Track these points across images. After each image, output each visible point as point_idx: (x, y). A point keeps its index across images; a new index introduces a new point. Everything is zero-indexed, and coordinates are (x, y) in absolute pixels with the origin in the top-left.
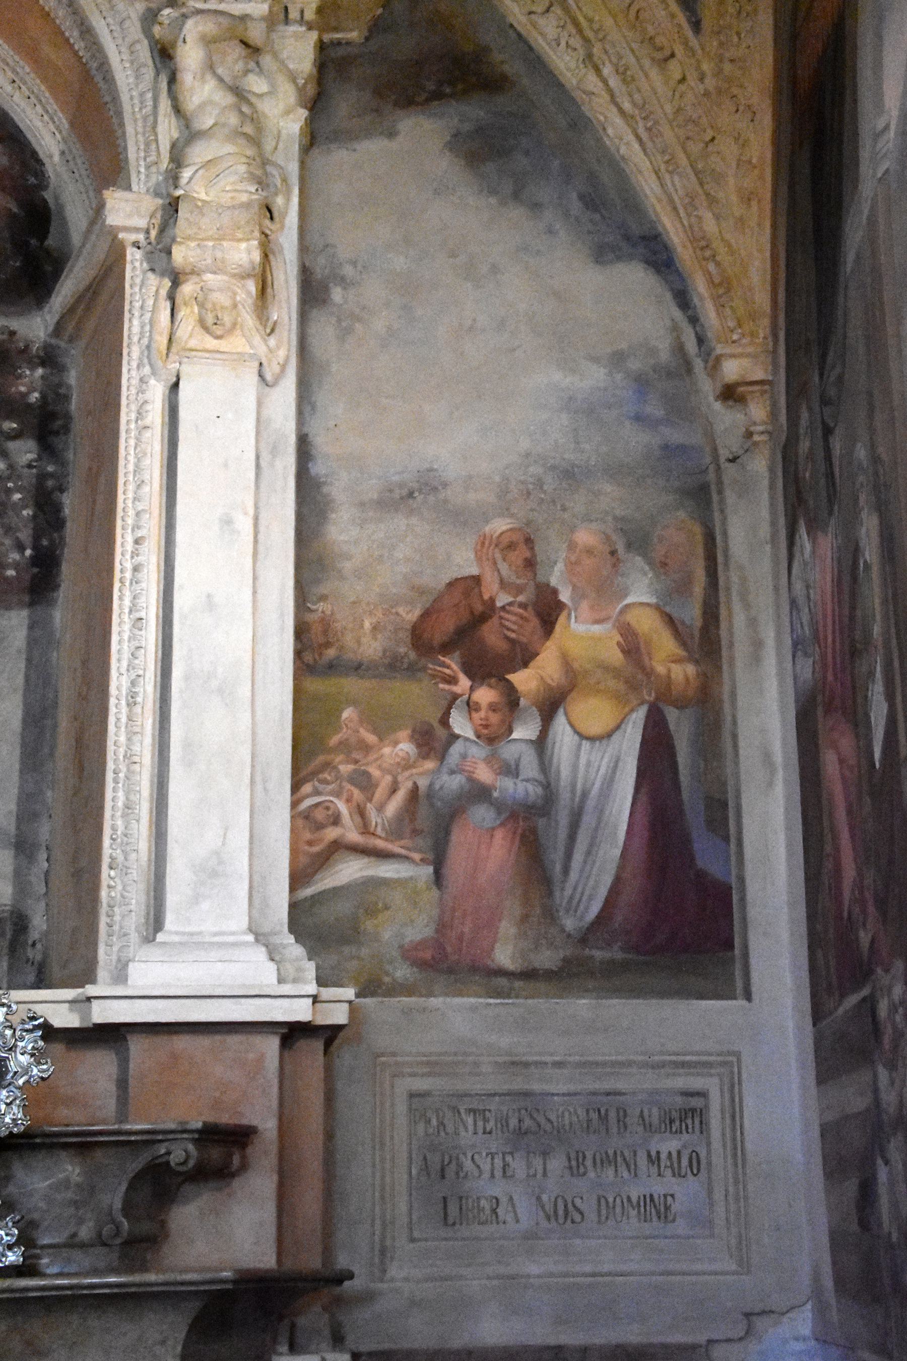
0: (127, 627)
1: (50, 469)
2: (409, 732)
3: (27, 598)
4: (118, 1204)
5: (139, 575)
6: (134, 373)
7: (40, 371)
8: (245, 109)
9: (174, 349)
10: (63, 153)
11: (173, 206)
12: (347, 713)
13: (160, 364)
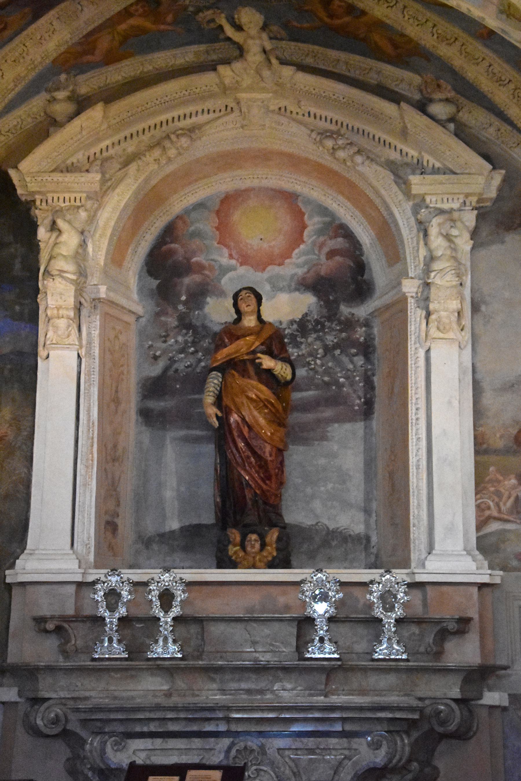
0: (415, 440)
1: (369, 367)
2: (514, 476)
3: (362, 417)
4: (431, 641)
5: (418, 422)
6: (413, 346)
7: (364, 329)
8: (452, 246)
9: (429, 338)
10: (371, 244)
11: (427, 285)
12: (492, 469)
13: (423, 344)
